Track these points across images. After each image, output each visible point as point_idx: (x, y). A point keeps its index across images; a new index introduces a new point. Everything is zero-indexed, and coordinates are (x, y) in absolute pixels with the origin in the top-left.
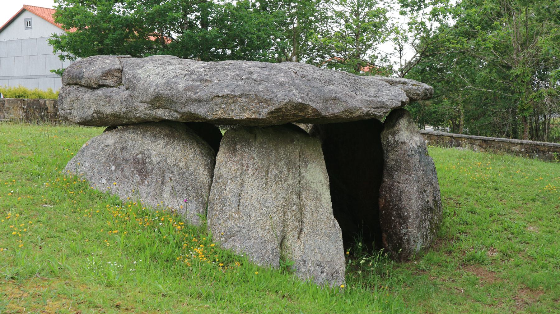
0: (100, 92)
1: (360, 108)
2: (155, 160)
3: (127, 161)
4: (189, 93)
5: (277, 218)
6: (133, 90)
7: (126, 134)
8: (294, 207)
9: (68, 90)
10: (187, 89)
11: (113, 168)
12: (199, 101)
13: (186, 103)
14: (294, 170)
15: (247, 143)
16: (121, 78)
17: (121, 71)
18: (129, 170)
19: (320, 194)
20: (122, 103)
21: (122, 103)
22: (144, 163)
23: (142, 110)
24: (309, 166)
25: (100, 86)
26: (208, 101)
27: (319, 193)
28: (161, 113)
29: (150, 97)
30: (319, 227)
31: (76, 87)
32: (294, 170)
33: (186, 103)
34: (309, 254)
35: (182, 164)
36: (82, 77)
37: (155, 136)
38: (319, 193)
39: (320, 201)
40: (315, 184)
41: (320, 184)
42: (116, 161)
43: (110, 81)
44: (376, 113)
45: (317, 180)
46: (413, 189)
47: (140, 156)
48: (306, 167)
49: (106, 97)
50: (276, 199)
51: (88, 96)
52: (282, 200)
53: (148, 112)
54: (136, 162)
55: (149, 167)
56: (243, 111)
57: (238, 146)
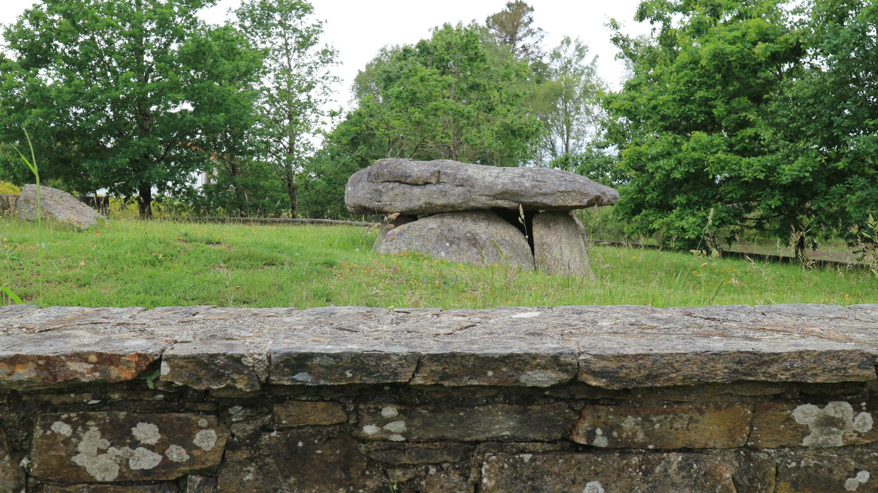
0: (429, 188)
2: (484, 237)
3: (459, 239)
4: (536, 190)
6: (472, 186)
7: (445, 220)
9: (390, 186)
10: (534, 186)
11: (448, 244)
12: (545, 194)
13: (534, 196)
15: (556, 222)
16: (439, 177)
17: (439, 172)
18: (464, 245)
20: (459, 196)
21: (459, 196)
22: (475, 239)
23: (484, 201)
25: (426, 183)
26: (552, 194)
28: (501, 203)
29: (493, 193)
31: (397, 184)
33: (534, 196)
35: (507, 238)
36: (410, 176)
37: (474, 220)
42: (441, 238)
43: (433, 180)
47: (468, 235)
49: (441, 191)
51: (417, 190)
53: (489, 202)
54: (469, 239)
55: (481, 242)
56: (573, 201)
57: (551, 224)
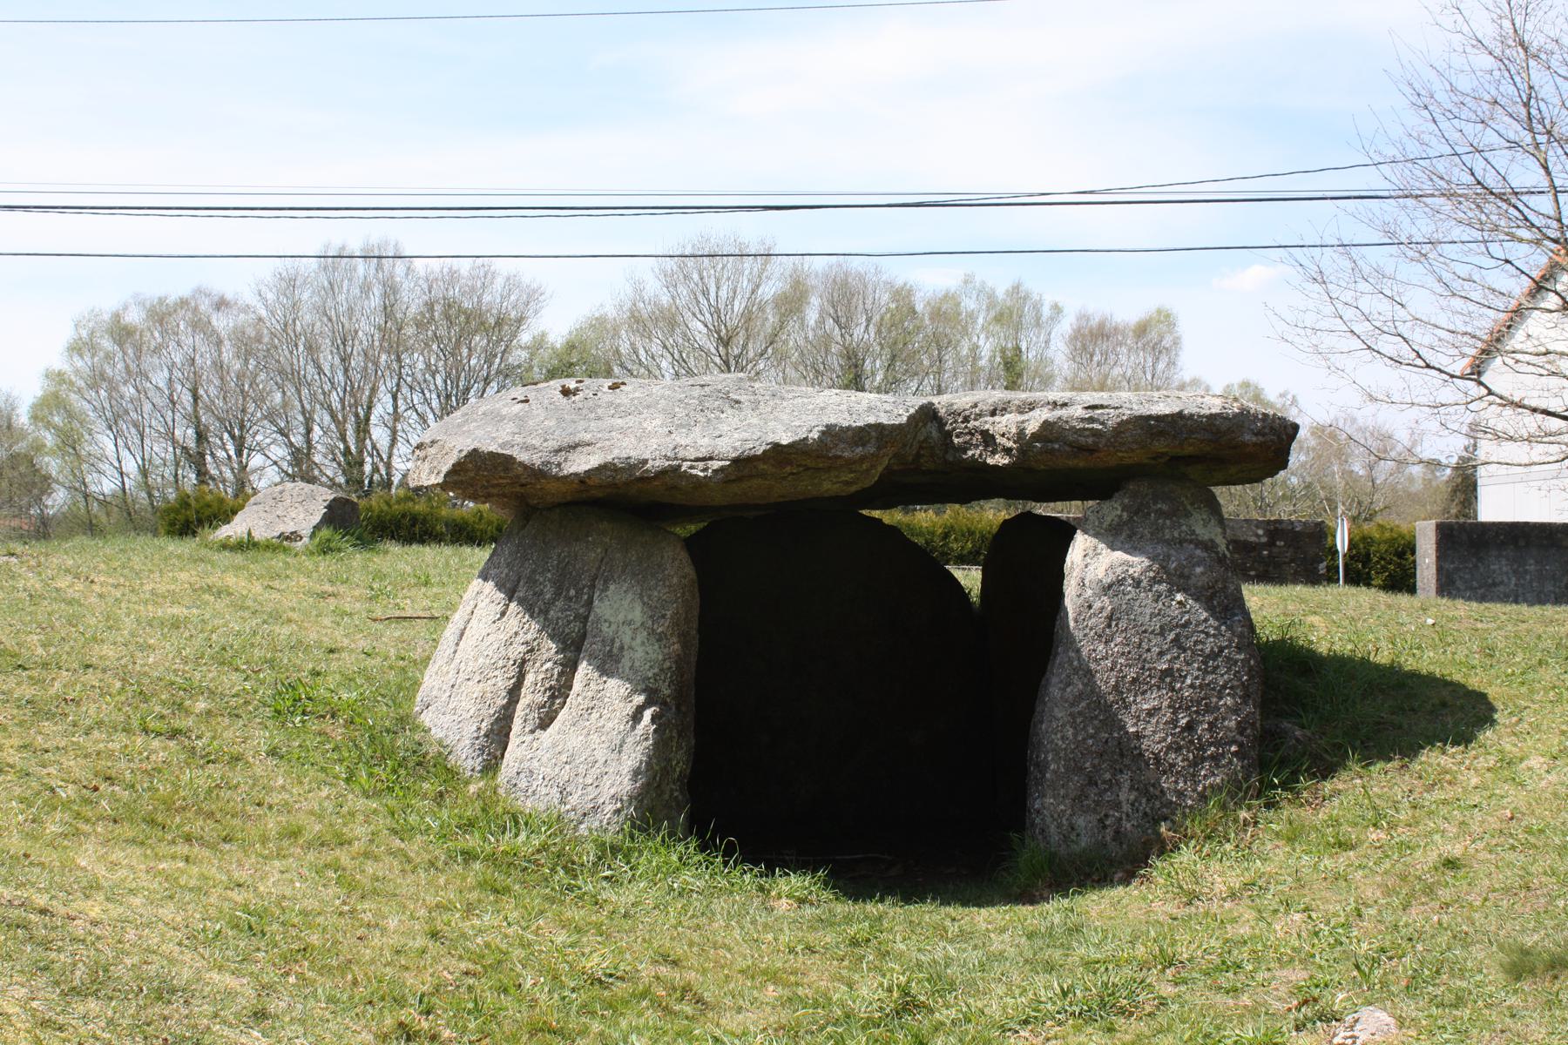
1: (645, 462)
5: (503, 683)
8: (549, 665)
14: (572, 592)
19: (622, 648)
24: (612, 587)
27: (617, 645)
30: (595, 715)
32: (572, 592)
34: (544, 759)
38: (617, 645)
39: (618, 662)
40: (614, 627)
41: (627, 628)
44: (694, 472)
45: (621, 617)
46: (1064, 690)
48: (606, 589)
50: (509, 643)
52: (523, 649)
